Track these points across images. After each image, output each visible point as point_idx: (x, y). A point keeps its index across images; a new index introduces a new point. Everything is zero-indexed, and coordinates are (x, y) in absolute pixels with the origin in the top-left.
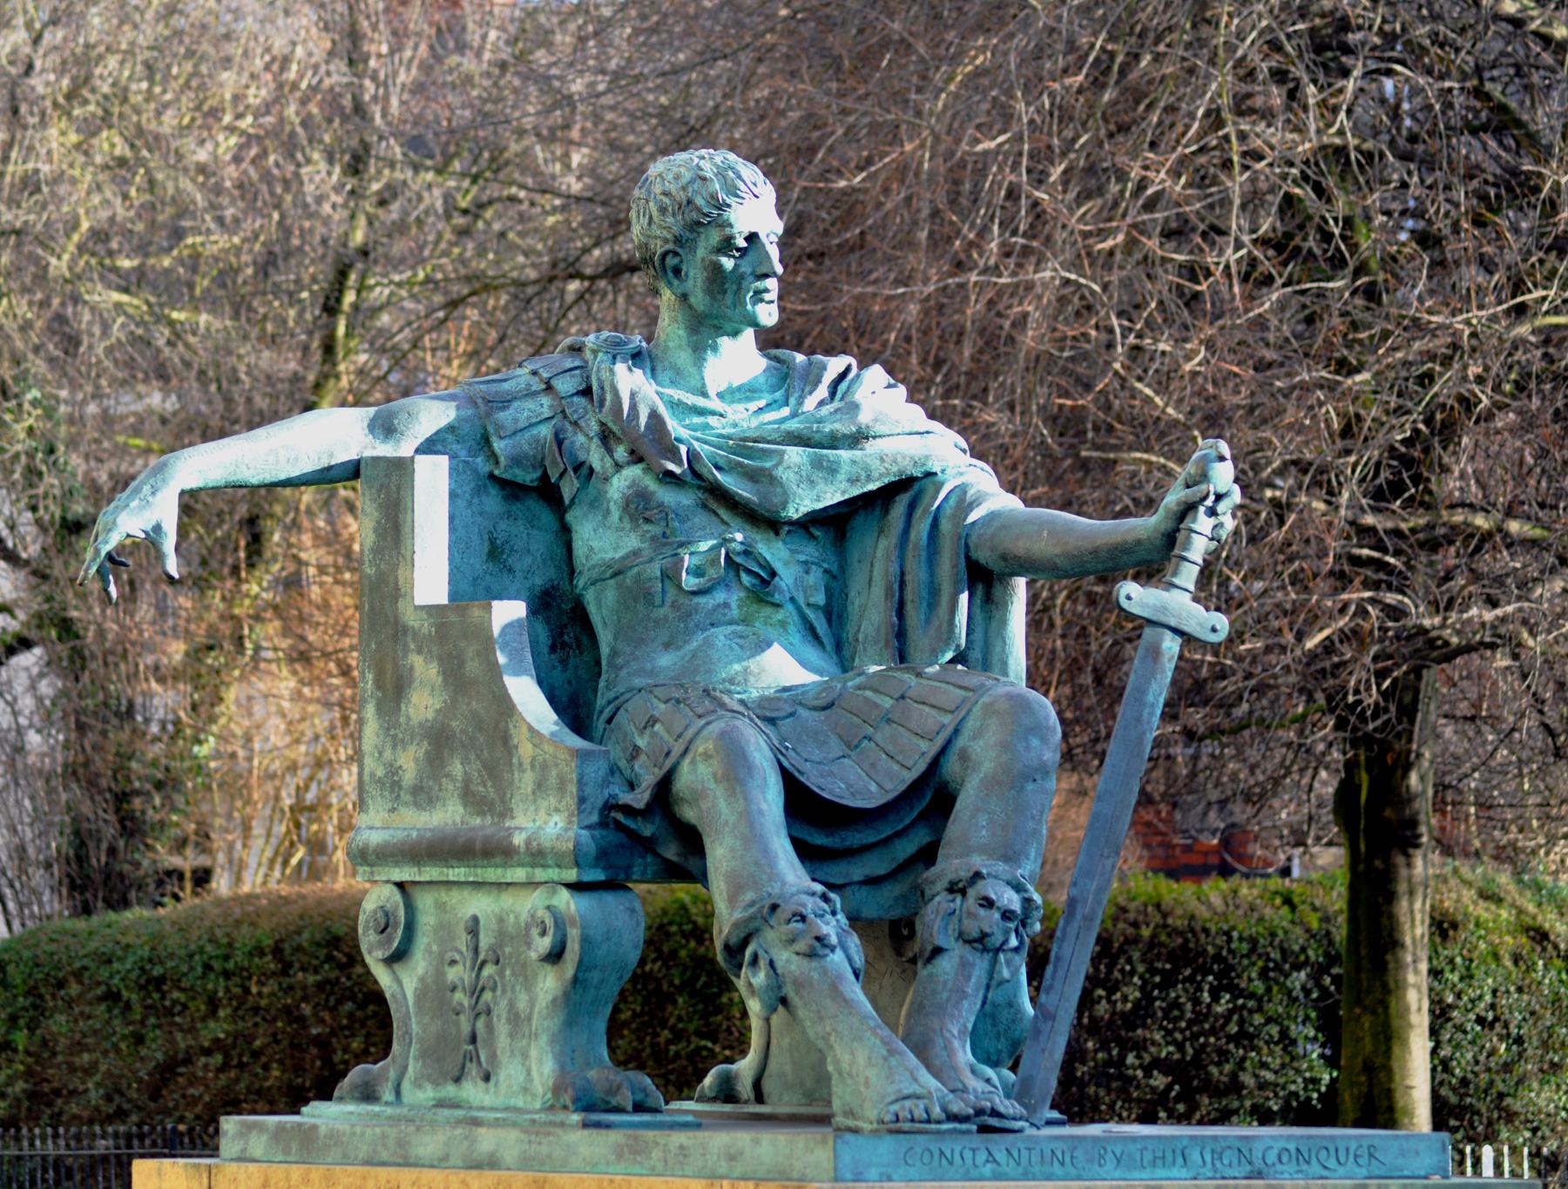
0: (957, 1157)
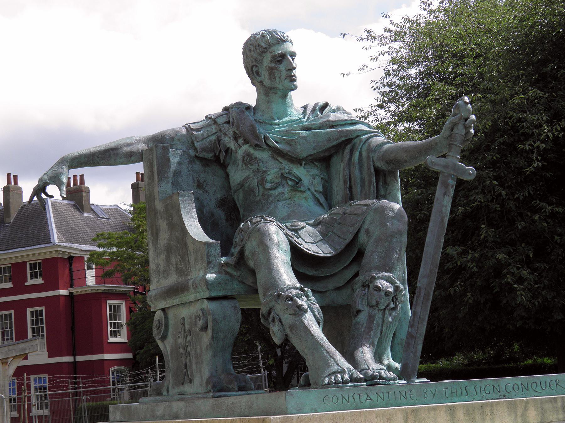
0: (351, 398)
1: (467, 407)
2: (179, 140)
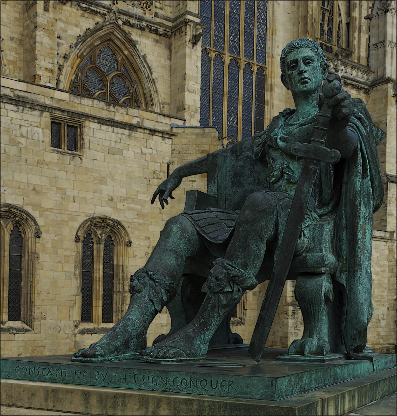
0: (36, 371)
1: (101, 395)
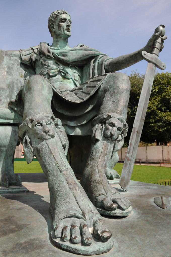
2: (14, 55)
